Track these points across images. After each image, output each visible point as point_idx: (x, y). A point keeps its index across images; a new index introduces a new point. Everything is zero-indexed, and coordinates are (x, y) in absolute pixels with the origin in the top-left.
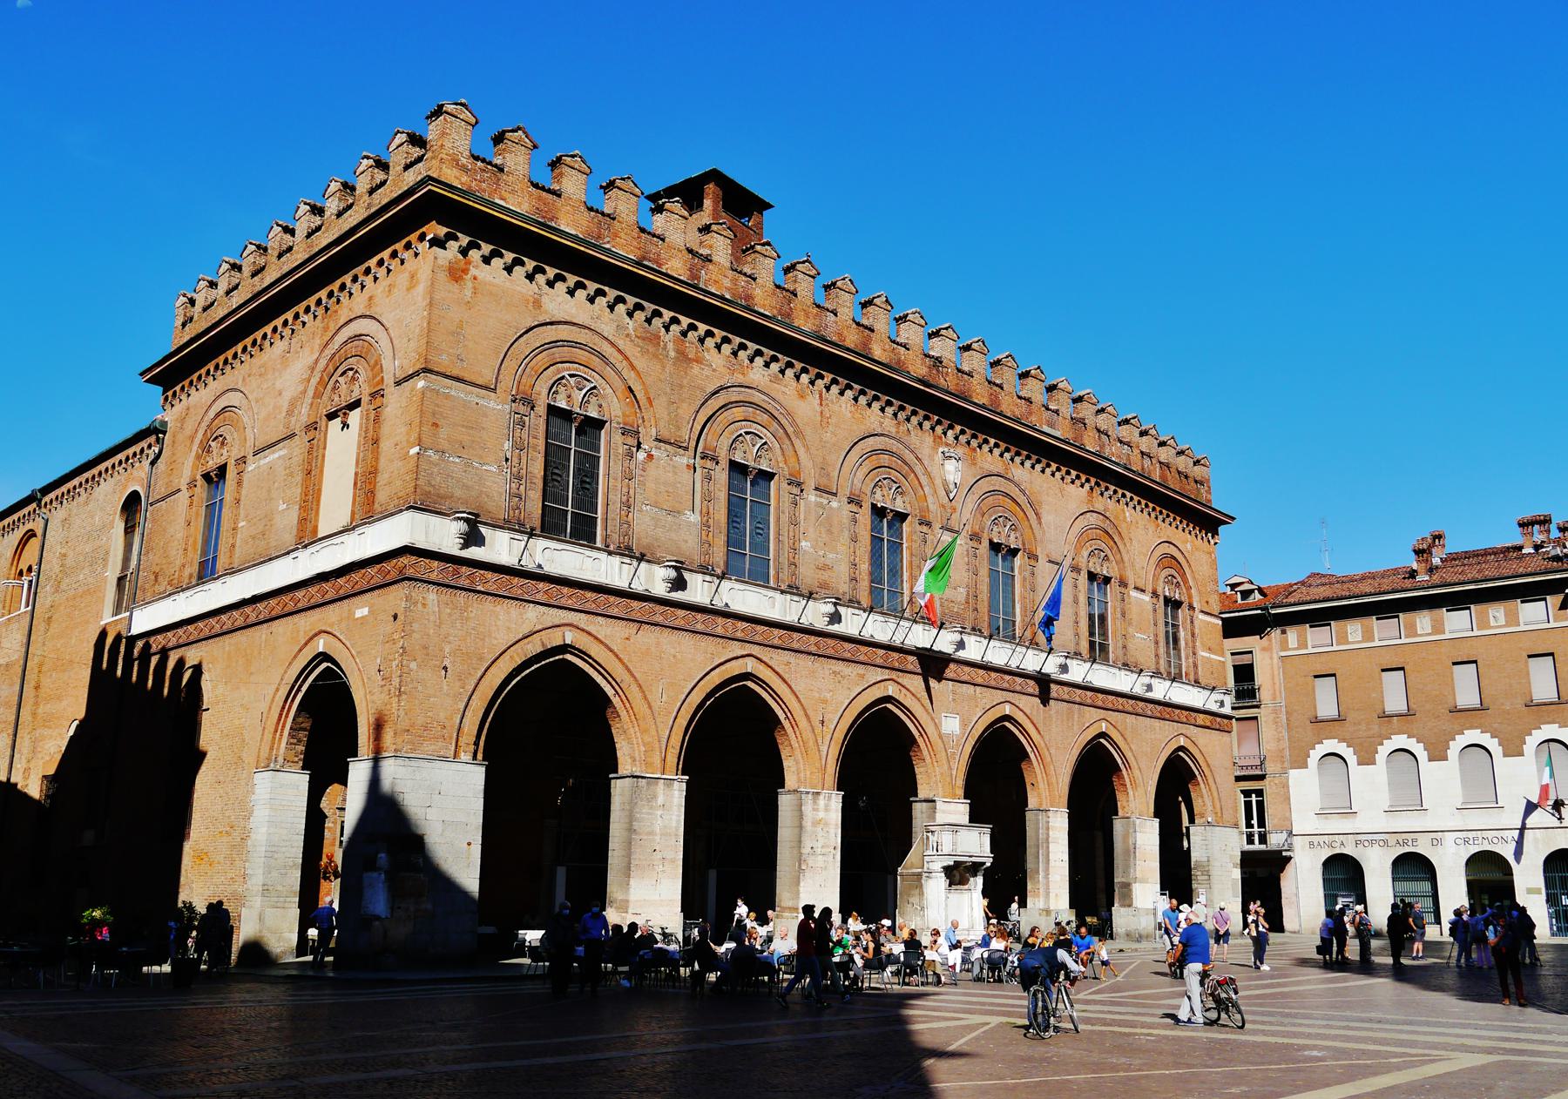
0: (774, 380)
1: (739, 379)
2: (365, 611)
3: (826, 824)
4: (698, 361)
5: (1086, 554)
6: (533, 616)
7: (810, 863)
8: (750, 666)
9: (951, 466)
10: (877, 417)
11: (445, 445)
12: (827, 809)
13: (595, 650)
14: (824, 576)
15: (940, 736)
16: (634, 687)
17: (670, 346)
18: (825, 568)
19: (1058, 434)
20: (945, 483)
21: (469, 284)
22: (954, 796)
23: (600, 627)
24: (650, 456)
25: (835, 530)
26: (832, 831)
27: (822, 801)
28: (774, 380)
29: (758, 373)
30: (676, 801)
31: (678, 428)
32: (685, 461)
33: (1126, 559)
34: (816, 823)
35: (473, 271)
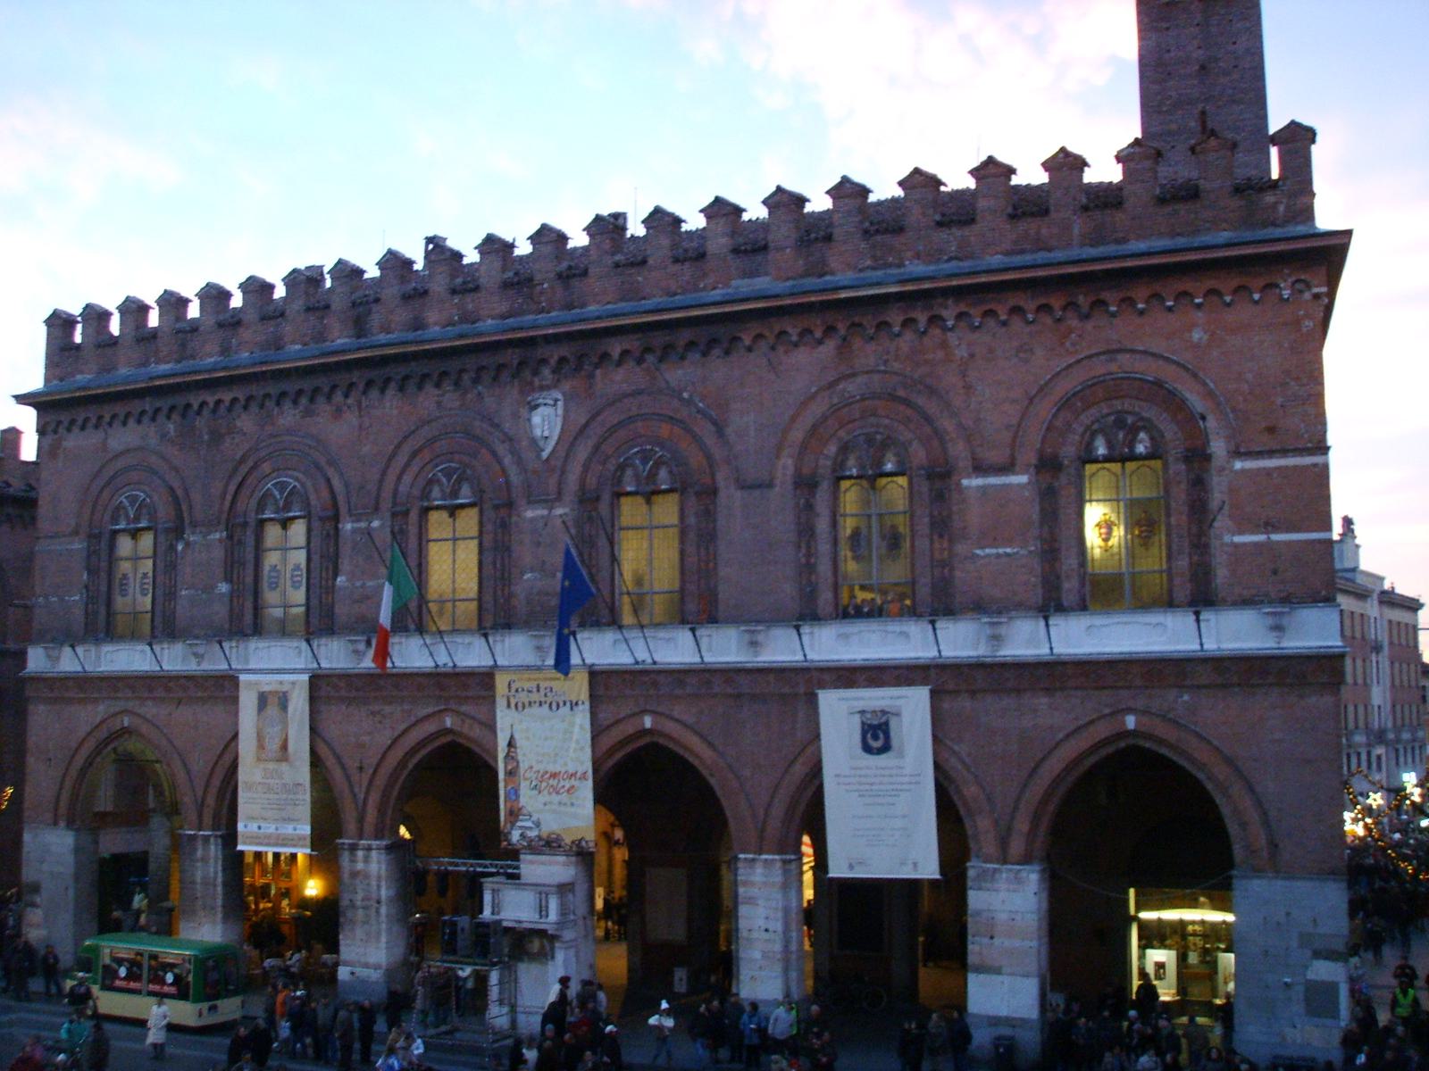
0: (308, 413)
1: (269, 429)
3: (367, 876)
5: (832, 449)
6: (101, 710)
7: (349, 914)
9: (536, 419)
10: (426, 400)
16: (176, 756)
19: (762, 283)
20: (533, 441)
23: (150, 710)
24: (188, 544)
26: (374, 883)
27: (360, 854)
29: (288, 417)
32: (217, 536)
33: (947, 424)
34: (354, 874)
35: (65, 444)
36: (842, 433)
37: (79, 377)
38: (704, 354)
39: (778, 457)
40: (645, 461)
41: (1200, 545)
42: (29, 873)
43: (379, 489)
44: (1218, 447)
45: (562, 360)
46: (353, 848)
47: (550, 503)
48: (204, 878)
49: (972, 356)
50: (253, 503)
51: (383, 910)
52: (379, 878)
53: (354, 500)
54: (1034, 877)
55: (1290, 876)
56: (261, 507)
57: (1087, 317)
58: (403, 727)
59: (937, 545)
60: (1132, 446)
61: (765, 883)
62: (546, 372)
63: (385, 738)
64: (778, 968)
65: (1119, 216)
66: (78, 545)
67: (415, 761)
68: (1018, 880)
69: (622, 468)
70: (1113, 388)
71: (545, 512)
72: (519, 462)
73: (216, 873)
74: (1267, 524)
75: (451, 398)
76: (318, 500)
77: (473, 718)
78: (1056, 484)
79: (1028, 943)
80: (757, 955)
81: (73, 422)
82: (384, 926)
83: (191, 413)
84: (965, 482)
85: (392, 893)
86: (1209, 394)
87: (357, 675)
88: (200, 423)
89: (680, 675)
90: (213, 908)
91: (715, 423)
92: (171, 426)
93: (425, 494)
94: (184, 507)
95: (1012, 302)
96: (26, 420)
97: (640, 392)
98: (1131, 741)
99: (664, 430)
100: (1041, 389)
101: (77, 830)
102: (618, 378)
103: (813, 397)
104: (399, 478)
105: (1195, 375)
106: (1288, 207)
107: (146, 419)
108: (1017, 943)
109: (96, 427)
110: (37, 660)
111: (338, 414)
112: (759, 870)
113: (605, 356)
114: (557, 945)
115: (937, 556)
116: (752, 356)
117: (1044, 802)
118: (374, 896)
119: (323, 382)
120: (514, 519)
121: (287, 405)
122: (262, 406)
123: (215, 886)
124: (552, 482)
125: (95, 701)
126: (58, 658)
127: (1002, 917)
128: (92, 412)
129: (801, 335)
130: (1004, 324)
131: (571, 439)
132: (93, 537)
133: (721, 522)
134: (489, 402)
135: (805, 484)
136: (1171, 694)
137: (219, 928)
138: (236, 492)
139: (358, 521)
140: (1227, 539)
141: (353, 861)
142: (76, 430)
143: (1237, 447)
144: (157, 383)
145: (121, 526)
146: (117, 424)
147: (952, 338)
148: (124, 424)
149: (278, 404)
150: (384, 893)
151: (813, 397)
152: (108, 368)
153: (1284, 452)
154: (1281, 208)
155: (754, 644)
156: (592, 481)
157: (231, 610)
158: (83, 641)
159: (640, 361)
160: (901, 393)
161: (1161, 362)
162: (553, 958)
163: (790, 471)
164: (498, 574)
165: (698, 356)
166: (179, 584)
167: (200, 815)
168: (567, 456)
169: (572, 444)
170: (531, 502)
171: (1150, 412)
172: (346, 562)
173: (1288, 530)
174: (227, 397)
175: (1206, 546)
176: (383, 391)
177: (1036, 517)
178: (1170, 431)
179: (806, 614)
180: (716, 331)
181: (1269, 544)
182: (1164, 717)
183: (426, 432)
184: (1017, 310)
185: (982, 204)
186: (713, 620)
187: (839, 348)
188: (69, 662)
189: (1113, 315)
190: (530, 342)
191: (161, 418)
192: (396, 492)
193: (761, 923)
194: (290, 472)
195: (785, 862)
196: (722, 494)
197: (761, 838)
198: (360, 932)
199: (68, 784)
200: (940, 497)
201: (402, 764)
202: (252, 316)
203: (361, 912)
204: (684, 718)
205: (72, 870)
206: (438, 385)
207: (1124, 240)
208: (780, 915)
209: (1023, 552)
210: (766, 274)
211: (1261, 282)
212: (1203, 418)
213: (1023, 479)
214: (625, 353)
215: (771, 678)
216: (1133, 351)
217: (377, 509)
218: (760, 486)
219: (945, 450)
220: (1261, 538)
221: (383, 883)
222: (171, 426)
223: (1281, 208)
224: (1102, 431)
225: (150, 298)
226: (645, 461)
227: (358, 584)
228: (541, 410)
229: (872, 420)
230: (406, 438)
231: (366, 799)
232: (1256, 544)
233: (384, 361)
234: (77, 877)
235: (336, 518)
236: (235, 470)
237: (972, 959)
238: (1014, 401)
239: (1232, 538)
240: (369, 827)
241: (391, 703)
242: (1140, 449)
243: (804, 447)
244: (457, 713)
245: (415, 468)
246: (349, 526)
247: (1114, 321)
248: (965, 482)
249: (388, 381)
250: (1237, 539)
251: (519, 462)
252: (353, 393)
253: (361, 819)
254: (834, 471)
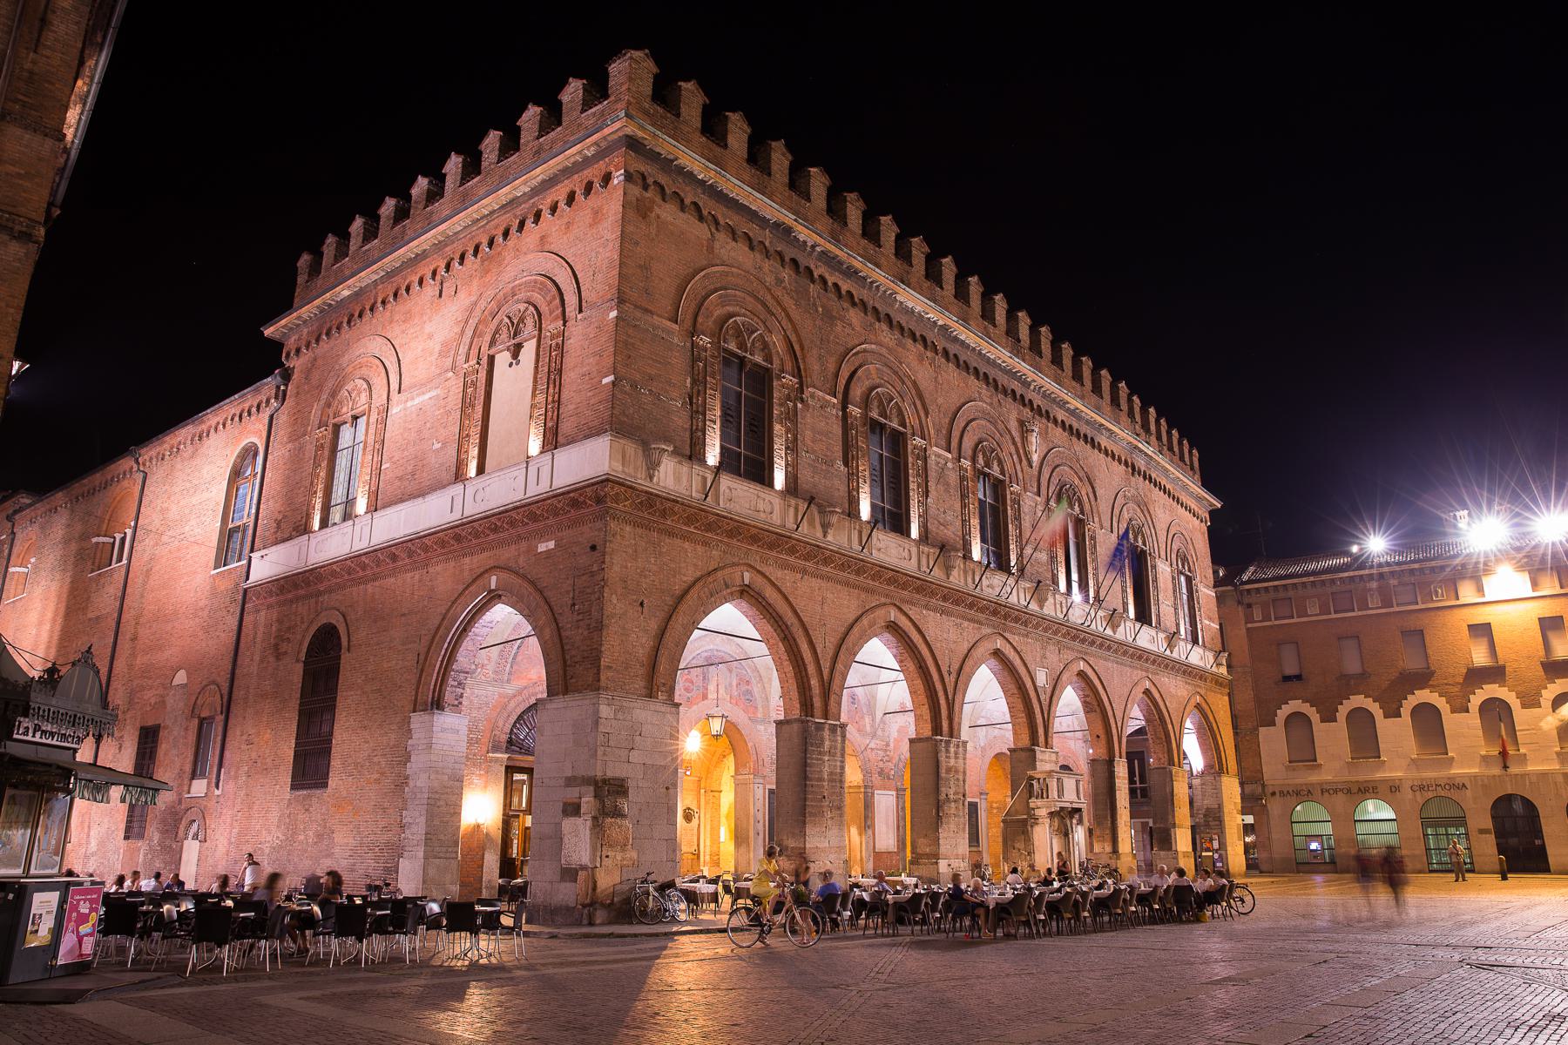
0: (900, 344)
2: (551, 545)
28: (900, 344)
34: (949, 770)
35: (657, 210)
46: (948, 743)
75: (985, 392)
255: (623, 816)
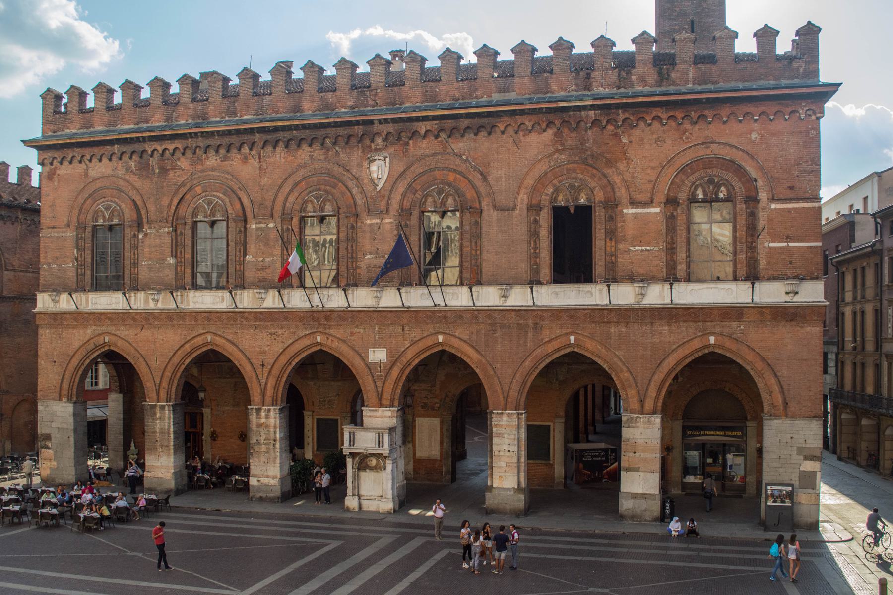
0: (225, 158)
3: (267, 426)
4: (174, 168)
5: (550, 190)
7: (256, 448)
8: (209, 338)
10: (304, 153)
11: (50, 260)
12: (267, 417)
13: (120, 343)
14: (263, 274)
15: (367, 365)
16: (141, 360)
17: (156, 167)
18: (264, 268)
19: (512, 96)
20: (372, 180)
21: (56, 179)
22: (381, 405)
23: (123, 332)
24: (146, 234)
25: (272, 243)
26: (272, 430)
27: (263, 414)
29: (212, 160)
30: (167, 416)
31: (161, 212)
32: (166, 230)
33: (617, 180)
34: (259, 426)
35: (58, 172)
36: (555, 182)
37: (68, 131)
38: (476, 135)
39: (518, 193)
40: (439, 193)
41: (752, 248)
42: (42, 430)
43: (273, 205)
44: (763, 196)
45: (389, 133)
46: (258, 410)
47: (381, 214)
48: (162, 429)
49: (630, 142)
50: (190, 210)
51: (278, 445)
52: (275, 427)
53: (256, 211)
54: (659, 421)
55: (794, 417)
56: (195, 214)
57: (696, 123)
58: (291, 341)
59: (608, 244)
60: (717, 194)
61: (508, 426)
62: (379, 141)
63: (278, 348)
64: (516, 471)
65: (715, 68)
66: (70, 233)
67: (297, 360)
68: (649, 422)
69: (426, 197)
70: (706, 163)
71: (378, 221)
72: (363, 192)
73: (169, 426)
74: (787, 238)
75: (318, 153)
76: (233, 210)
77: (334, 336)
78: (675, 213)
79: (654, 455)
80: (504, 464)
81: (63, 158)
82: (278, 454)
83: (145, 156)
84: (625, 211)
85: (282, 435)
86: (761, 168)
87: (262, 313)
88: (153, 161)
89: (460, 314)
90: (168, 446)
91: (482, 174)
92: (132, 164)
93: (303, 209)
94: (143, 212)
95: (654, 114)
96: (31, 158)
97: (435, 154)
98: (711, 349)
99: (451, 177)
100: (669, 161)
101: (75, 403)
102: (424, 146)
103: (540, 161)
104: (286, 199)
105: (752, 157)
106: (805, 70)
107: (114, 158)
108: (647, 455)
109: (80, 162)
110: (44, 302)
111: (245, 160)
112: (505, 419)
113: (415, 133)
114: (388, 461)
115: (608, 249)
116: (504, 136)
117: (664, 381)
118: (272, 436)
119: (234, 139)
120: (359, 224)
121: (212, 152)
122: (195, 153)
123: (169, 433)
124: (383, 204)
125: (85, 327)
126: (58, 301)
127: (641, 441)
128: (77, 152)
129: (533, 126)
130: (650, 125)
131: (394, 179)
132: (81, 227)
133: (485, 229)
134: (343, 156)
135: (534, 208)
136: (734, 324)
137: (172, 458)
138: (178, 204)
139: (260, 223)
140: (766, 245)
141: (259, 417)
142: (66, 163)
143: (773, 196)
144: (124, 136)
145: (101, 222)
146: (95, 161)
147: (619, 131)
148: (100, 160)
149: (206, 153)
150: (278, 436)
151: (540, 161)
152: (89, 125)
153: (798, 200)
154: (801, 70)
155: (505, 296)
156: (407, 204)
157: (177, 273)
158: (76, 291)
159: (437, 137)
160: (590, 161)
161: (734, 150)
162: (385, 469)
163: (526, 202)
164: (350, 255)
165: (472, 135)
166: (140, 258)
167: (158, 394)
168: (391, 191)
169: (395, 183)
170: (369, 212)
171: (729, 176)
172: (252, 247)
173: (798, 241)
174: (171, 146)
175: (755, 248)
176: (275, 147)
177: (664, 231)
178: (738, 185)
179: (534, 281)
180: (484, 122)
181: (788, 247)
182: (730, 337)
183: (302, 172)
184: (657, 118)
185: (638, 58)
186: (479, 283)
187: (555, 134)
188: (65, 303)
189: (710, 123)
190: (371, 122)
191: (126, 158)
192: (284, 205)
193: (506, 447)
194: (215, 193)
195: (518, 414)
196: (485, 214)
197: (506, 401)
198: (263, 459)
199: (68, 376)
200: (611, 218)
201: (289, 362)
202: (186, 99)
203: (263, 446)
204: (461, 336)
205: (72, 427)
206: (310, 145)
207: (716, 83)
208: (516, 442)
209: (656, 249)
210: (514, 91)
211: (790, 109)
212: (756, 181)
213: (657, 210)
214: (427, 131)
215: (513, 314)
216: (719, 143)
217: (272, 216)
218: (508, 209)
219: (614, 192)
220: (785, 245)
221: (278, 430)
222: (132, 164)
223: (801, 70)
224: (701, 185)
225: (115, 84)
226: (439, 193)
227: (260, 260)
228: (377, 162)
229: (574, 175)
230: (290, 175)
231: (266, 384)
232: (781, 248)
233: (276, 129)
234: (75, 430)
235: (246, 221)
236: (178, 190)
237: (624, 464)
238: (653, 168)
239: (768, 244)
240: (268, 399)
241: (282, 328)
242: (721, 196)
243: (534, 190)
244: (326, 333)
245: (296, 194)
246: (254, 226)
247: (711, 127)
248: (625, 211)
249: (277, 141)
250: (771, 245)
251: (363, 192)
252: (255, 148)
253: (263, 394)
254: (551, 202)
255: (47, 447)
